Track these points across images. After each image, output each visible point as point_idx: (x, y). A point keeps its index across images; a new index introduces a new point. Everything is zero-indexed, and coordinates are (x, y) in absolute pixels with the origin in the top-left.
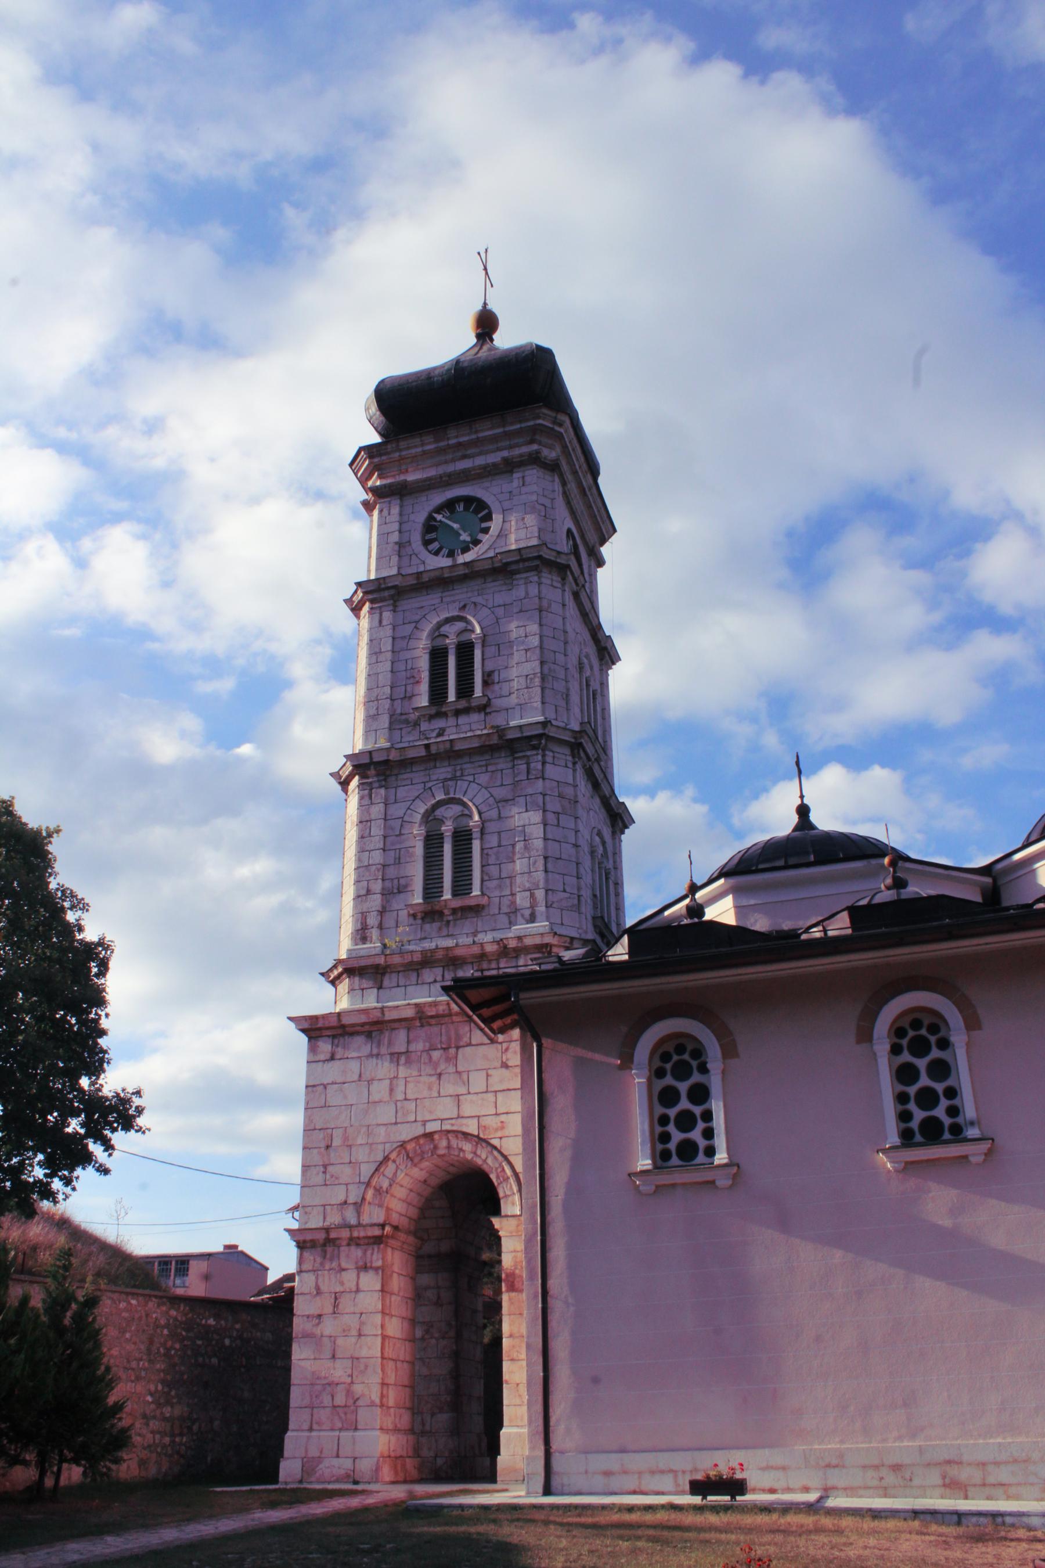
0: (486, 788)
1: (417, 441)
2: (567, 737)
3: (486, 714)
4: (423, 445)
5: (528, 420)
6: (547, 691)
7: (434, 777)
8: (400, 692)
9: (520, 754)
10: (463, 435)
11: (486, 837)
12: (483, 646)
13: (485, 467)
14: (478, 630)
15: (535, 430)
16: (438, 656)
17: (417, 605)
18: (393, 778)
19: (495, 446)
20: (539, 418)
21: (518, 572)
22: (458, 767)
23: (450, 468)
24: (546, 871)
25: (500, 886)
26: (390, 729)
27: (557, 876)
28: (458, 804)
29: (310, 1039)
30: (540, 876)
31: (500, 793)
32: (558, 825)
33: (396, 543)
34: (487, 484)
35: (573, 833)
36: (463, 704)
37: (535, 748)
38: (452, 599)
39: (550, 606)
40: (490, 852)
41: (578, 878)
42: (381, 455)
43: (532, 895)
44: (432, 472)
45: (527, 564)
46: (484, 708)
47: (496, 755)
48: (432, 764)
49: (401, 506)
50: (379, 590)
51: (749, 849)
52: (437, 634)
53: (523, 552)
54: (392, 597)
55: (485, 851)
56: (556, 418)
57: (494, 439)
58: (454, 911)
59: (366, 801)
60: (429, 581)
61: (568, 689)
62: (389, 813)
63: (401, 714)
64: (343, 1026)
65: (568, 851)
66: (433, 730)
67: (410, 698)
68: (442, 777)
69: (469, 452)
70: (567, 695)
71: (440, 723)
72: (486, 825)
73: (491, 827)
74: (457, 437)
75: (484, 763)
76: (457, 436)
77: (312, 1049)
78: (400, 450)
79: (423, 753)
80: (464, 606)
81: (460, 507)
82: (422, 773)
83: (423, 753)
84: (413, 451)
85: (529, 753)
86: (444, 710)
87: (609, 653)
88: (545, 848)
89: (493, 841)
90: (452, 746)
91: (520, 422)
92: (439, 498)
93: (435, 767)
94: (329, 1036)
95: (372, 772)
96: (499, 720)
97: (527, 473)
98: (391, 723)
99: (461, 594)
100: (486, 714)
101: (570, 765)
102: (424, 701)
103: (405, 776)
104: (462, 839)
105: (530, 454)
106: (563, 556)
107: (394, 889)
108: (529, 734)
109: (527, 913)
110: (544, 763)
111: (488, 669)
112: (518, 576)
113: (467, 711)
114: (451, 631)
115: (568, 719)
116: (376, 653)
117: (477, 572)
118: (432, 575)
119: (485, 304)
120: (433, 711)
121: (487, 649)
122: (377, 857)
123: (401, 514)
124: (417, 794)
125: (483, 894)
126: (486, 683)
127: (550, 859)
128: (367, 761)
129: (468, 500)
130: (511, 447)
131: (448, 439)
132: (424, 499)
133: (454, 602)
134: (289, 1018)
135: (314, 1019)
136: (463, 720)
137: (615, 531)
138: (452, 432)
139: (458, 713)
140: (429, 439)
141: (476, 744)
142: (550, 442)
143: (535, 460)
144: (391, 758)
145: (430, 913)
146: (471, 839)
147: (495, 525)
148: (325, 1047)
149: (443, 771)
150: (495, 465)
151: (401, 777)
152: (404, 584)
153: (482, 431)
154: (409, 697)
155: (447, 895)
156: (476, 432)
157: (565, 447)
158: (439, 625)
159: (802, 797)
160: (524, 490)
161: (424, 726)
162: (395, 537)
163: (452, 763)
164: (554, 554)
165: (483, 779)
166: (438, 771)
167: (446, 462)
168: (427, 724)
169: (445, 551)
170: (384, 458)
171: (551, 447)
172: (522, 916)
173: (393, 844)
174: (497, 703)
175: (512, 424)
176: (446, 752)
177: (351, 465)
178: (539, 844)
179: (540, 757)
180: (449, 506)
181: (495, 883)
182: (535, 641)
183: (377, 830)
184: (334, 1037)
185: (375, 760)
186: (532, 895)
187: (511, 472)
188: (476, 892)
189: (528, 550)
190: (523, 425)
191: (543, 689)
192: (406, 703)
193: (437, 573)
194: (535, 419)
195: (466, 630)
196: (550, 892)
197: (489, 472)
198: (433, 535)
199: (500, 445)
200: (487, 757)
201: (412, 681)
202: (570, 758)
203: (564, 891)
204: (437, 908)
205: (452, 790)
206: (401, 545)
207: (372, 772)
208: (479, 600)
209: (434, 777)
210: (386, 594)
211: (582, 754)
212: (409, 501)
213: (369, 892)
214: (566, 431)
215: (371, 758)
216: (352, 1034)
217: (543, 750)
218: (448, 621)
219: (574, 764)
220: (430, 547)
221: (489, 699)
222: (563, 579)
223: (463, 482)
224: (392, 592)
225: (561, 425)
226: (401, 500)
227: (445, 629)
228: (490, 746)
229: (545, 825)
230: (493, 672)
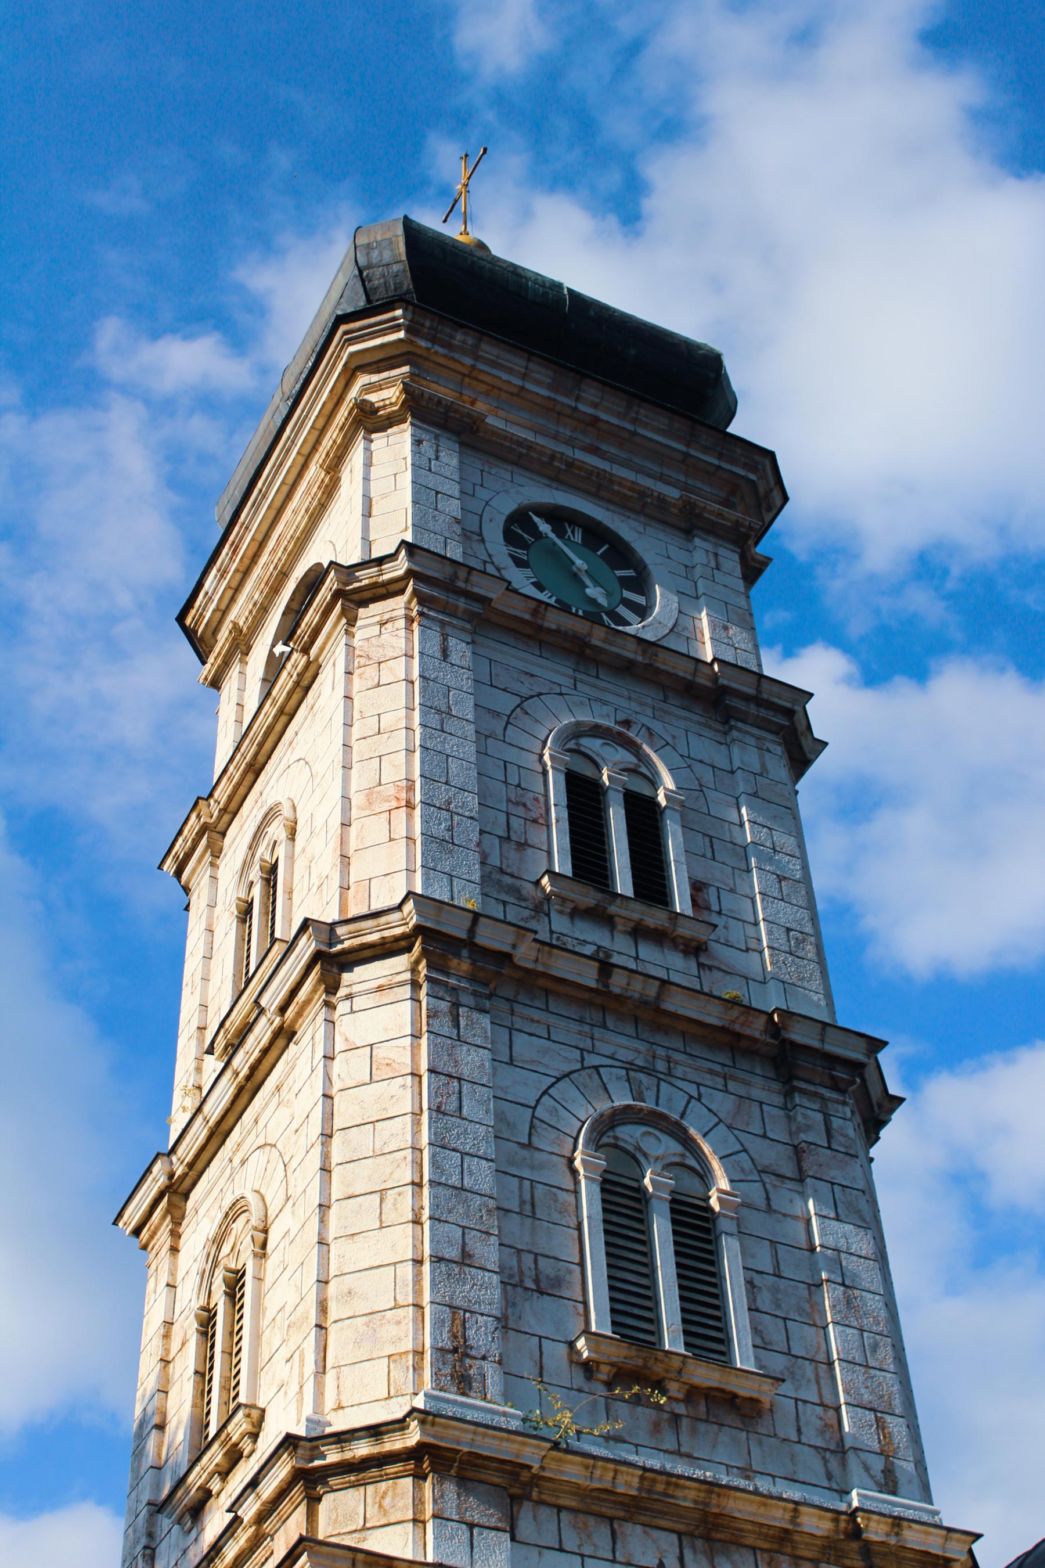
0: (730, 1127)
1: (518, 362)
5: (733, 461)
7: (607, 1049)
10: (607, 410)
13: (643, 493)
17: (520, 665)
19: (656, 469)
28: (671, 1134)
36: (655, 918)
42: (434, 340)
43: (880, 1425)
45: (763, 713)
48: (596, 1016)
50: (448, 586)
54: (471, 617)
58: (692, 1393)
60: (557, 631)
69: (604, 447)
74: (595, 406)
79: (588, 976)
80: (627, 723)
83: (588, 976)
84: (505, 376)
91: (720, 456)
95: (463, 965)
97: (722, 551)
100: (700, 965)
107: (532, 1281)
109: (877, 1464)
113: (659, 937)
117: (659, 671)
122: (482, 1177)
124: (567, 1068)
128: (463, 935)
129: (596, 535)
131: (578, 399)
133: (605, 703)
138: (591, 392)
139: (639, 932)
140: (542, 373)
141: (713, 1015)
149: (621, 1044)
152: (500, 608)
153: (646, 426)
156: (635, 421)
172: (867, 1469)
175: (706, 450)
176: (643, 1003)
185: (479, 940)
186: (880, 1425)
192: (512, 854)
194: (745, 466)
199: (666, 471)
201: (520, 811)
205: (650, 1095)
207: (463, 965)
208: (657, 726)
210: (462, 603)
215: (472, 931)
223: (590, 493)
227: (592, 745)
228: (738, 1036)
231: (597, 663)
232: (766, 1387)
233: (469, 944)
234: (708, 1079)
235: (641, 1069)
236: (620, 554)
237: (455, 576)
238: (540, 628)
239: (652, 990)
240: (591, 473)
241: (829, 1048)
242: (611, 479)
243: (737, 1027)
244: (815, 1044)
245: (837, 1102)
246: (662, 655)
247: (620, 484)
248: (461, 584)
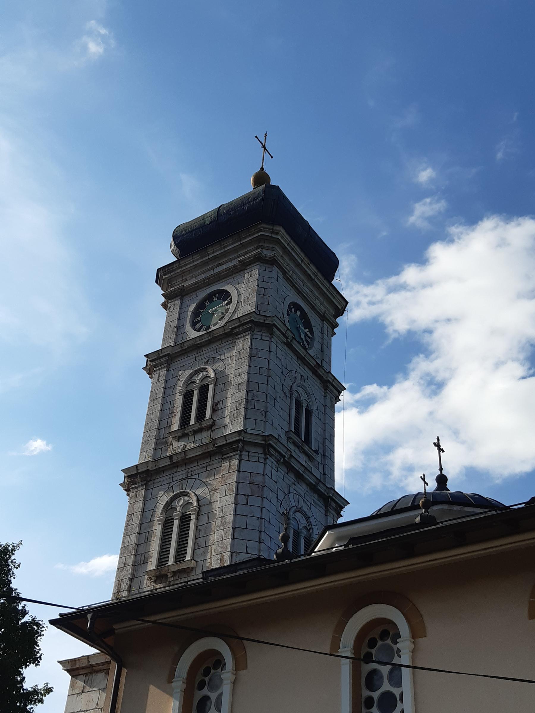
2: (259, 441)
3: (212, 431)
4: (194, 262)
5: (254, 234)
6: (249, 411)
7: (175, 479)
8: (164, 424)
9: (226, 456)
11: (200, 517)
12: (215, 386)
13: (229, 269)
14: (212, 375)
15: (260, 239)
16: (188, 396)
18: (151, 483)
20: (261, 231)
21: (237, 334)
22: (190, 469)
23: (212, 273)
24: (233, 539)
25: (204, 552)
26: (155, 449)
27: (242, 542)
29: (73, 676)
30: (228, 541)
32: (247, 504)
33: (175, 327)
34: (231, 280)
35: (259, 509)
37: (235, 450)
38: (201, 357)
39: (258, 353)
40: (201, 528)
41: (260, 542)
43: (222, 557)
44: (200, 278)
46: (211, 427)
47: (213, 459)
48: (175, 470)
49: (181, 303)
51: (380, 509)
52: (190, 382)
53: (241, 319)
55: (199, 528)
56: (273, 229)
57: (236, 250)
58: (174, 573)
59: (133, 501)
60: (188, 347)
61: (267, 408)
62: (146, 507)
63: (163, 438)
64: (92, 666)
65: (254, 522)
66: (180, 447)
67: (170, 426)
68: (181, 477)
70: (266, 412)
72: (202, 508)
73: (204, 510)
74: (213, 253)
75: (205, 465)
76: (214, 252)
77: (72, 686)
78: (181, 267)
81: (215, 298)
82: (169, 477)
84: (188, 266)
85: (231, 454)
86: (186, 432)
87: (332, 385)
88: (234, 521)
89: (204, 519)
90: (185, 456)
91: (250, 236)
92: (202, 294)
93: (177, 472)
94: (83, 674)
95: (138, 479)
96: (218, 434)
98: (156, 445)
99: (207, 353)
100: (212, 431)
101: (262, 460)
102: (175, 427)
103: (158, 480)
104: (185, 520)
105: (255, 255)
106: (269, 319)
108: (231, 441)
110: (240, 461)
111: (216, 401)
112: (239, 336)
114: (198, 379)
115: (265, 429)
116: (153, 400)
118: (189, 343)
119: (262, 169)
120: (180, 434)
121: (217, 387)
123: (180, 309)
125: (193, 558)
126: (214, 410)
127: (236, 530)
130: (246, 253)
131: (208, 255)
132: (195, 296)
134: (59, 662)
135: (74, 661)
136: (198, 437)
137: (347, 303)
138: (210, 251)
139: (195, 433)
140: (196, 257)
142: (271, 246)
143: (259, 259)
144: (149, 468)
146: (190, 520)
147: (232, 307)
148: (80, 684)
149: (181, 474)
150: (234, 266)
151: (156, 481)
153: (228, 246)
155: (171, 562)
156: (224, 247)
157: (284, 248)
158: (192, 376)
159: (441, 469)
160: (251, 279)
161: (176, 444)
162: (175, 324)
163: (187, 467)
164: (262, 318)
166: (178, 474)
167: (208, 270)
168: (177, 443)
169: (204, 327)
170: (172, 274)
171: (272, 249)
173: (145, 529)
174: (219, 422)
175: (245, 238)
176: (183, 460)
177: (156, 282)
178: (230, 518)
179: (238, 456)
180: (210, 298)
181: (202, 550)
182: (244, 378)
183: (136, 521)
184: (86, 674)
187: (245, 270)
188: (188, 558)
189: (244, 318)
190: (251, 238)
191: (246, 409)
193: (192, 342)
194: (258, 232)
196: (234, 554)
198: (199, 319)
200: (208, 460)
202: (262, 456)
203: (247, 553)
204: (163, 572)
206: (178, 327)
207: (138, 479)
209: (175, 479)
210: (163, 360)
211: (272, 452)
212: (186, 299)
213: (125, 564)
214: (282, 237)
215: (137, 470)
216: (97, 672)
217: (241, 451)
219: (265, 459)
220: (196, 327)
221: (214, 421)
222: (271, 334)
224: (167, 358)
225: (277, 234)
226: (182, 299)
229: (236, 504)
230: (219, 402)
231: (203, 347)
232: (189, 563)
233: (138, 473)
234: (202, 470)
235: (184, 479)
237: (159, 354)
238: (185, 350)
239: (183, 455)
240: (214, 276)
241: (228, 441)
242: (219, 273)
243: (206, 451)
244: (225, 443)
245: (234, 455)
246: (214, 332)
247: (223, 272)
248: (161, 355)
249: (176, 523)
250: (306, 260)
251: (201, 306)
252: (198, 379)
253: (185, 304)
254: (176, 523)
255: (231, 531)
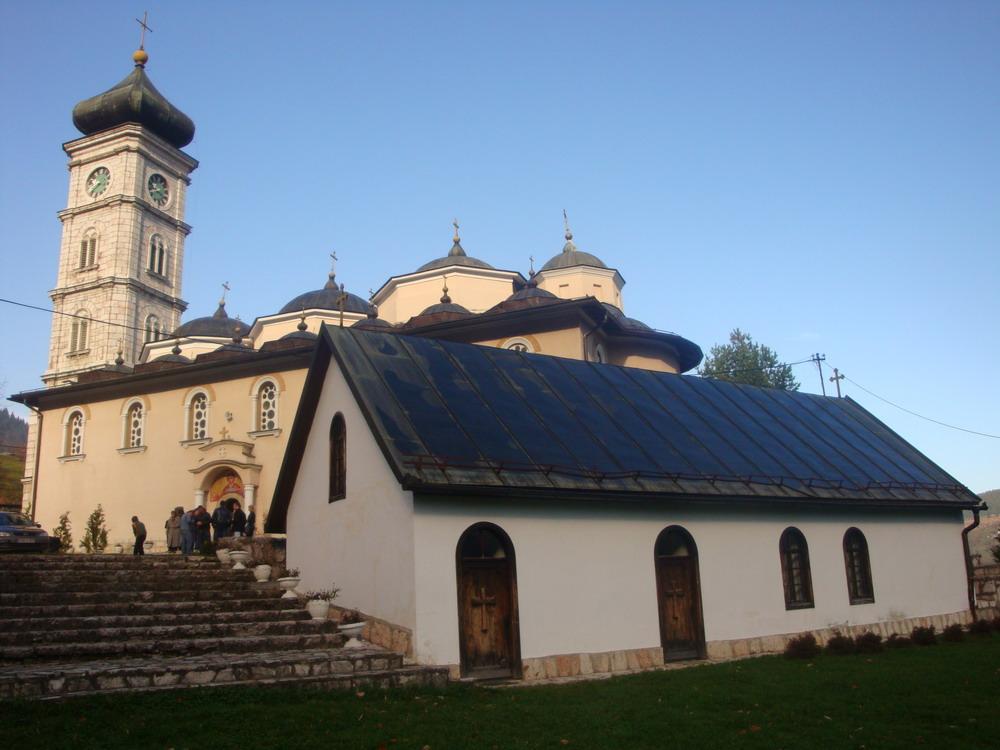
16: (84, 244)
31: (99, 306)
71: (83, 275)
102: (78, 266)
114: (90, 233)
126: (99, 258)
145: (72, 356)
154: (74, 264)
158: (86, 231)
165: (94, 300)
180: (98, 170)
195: (95, 233)
197: (109, 155)
218: (90, 229)
236: (104, 168)
249: (80, 327)
250: (163, 142)
251: (92, 176)
252: (90, 233)
253: (82, 173)
254: (80, 327)
255: (107, 335)
